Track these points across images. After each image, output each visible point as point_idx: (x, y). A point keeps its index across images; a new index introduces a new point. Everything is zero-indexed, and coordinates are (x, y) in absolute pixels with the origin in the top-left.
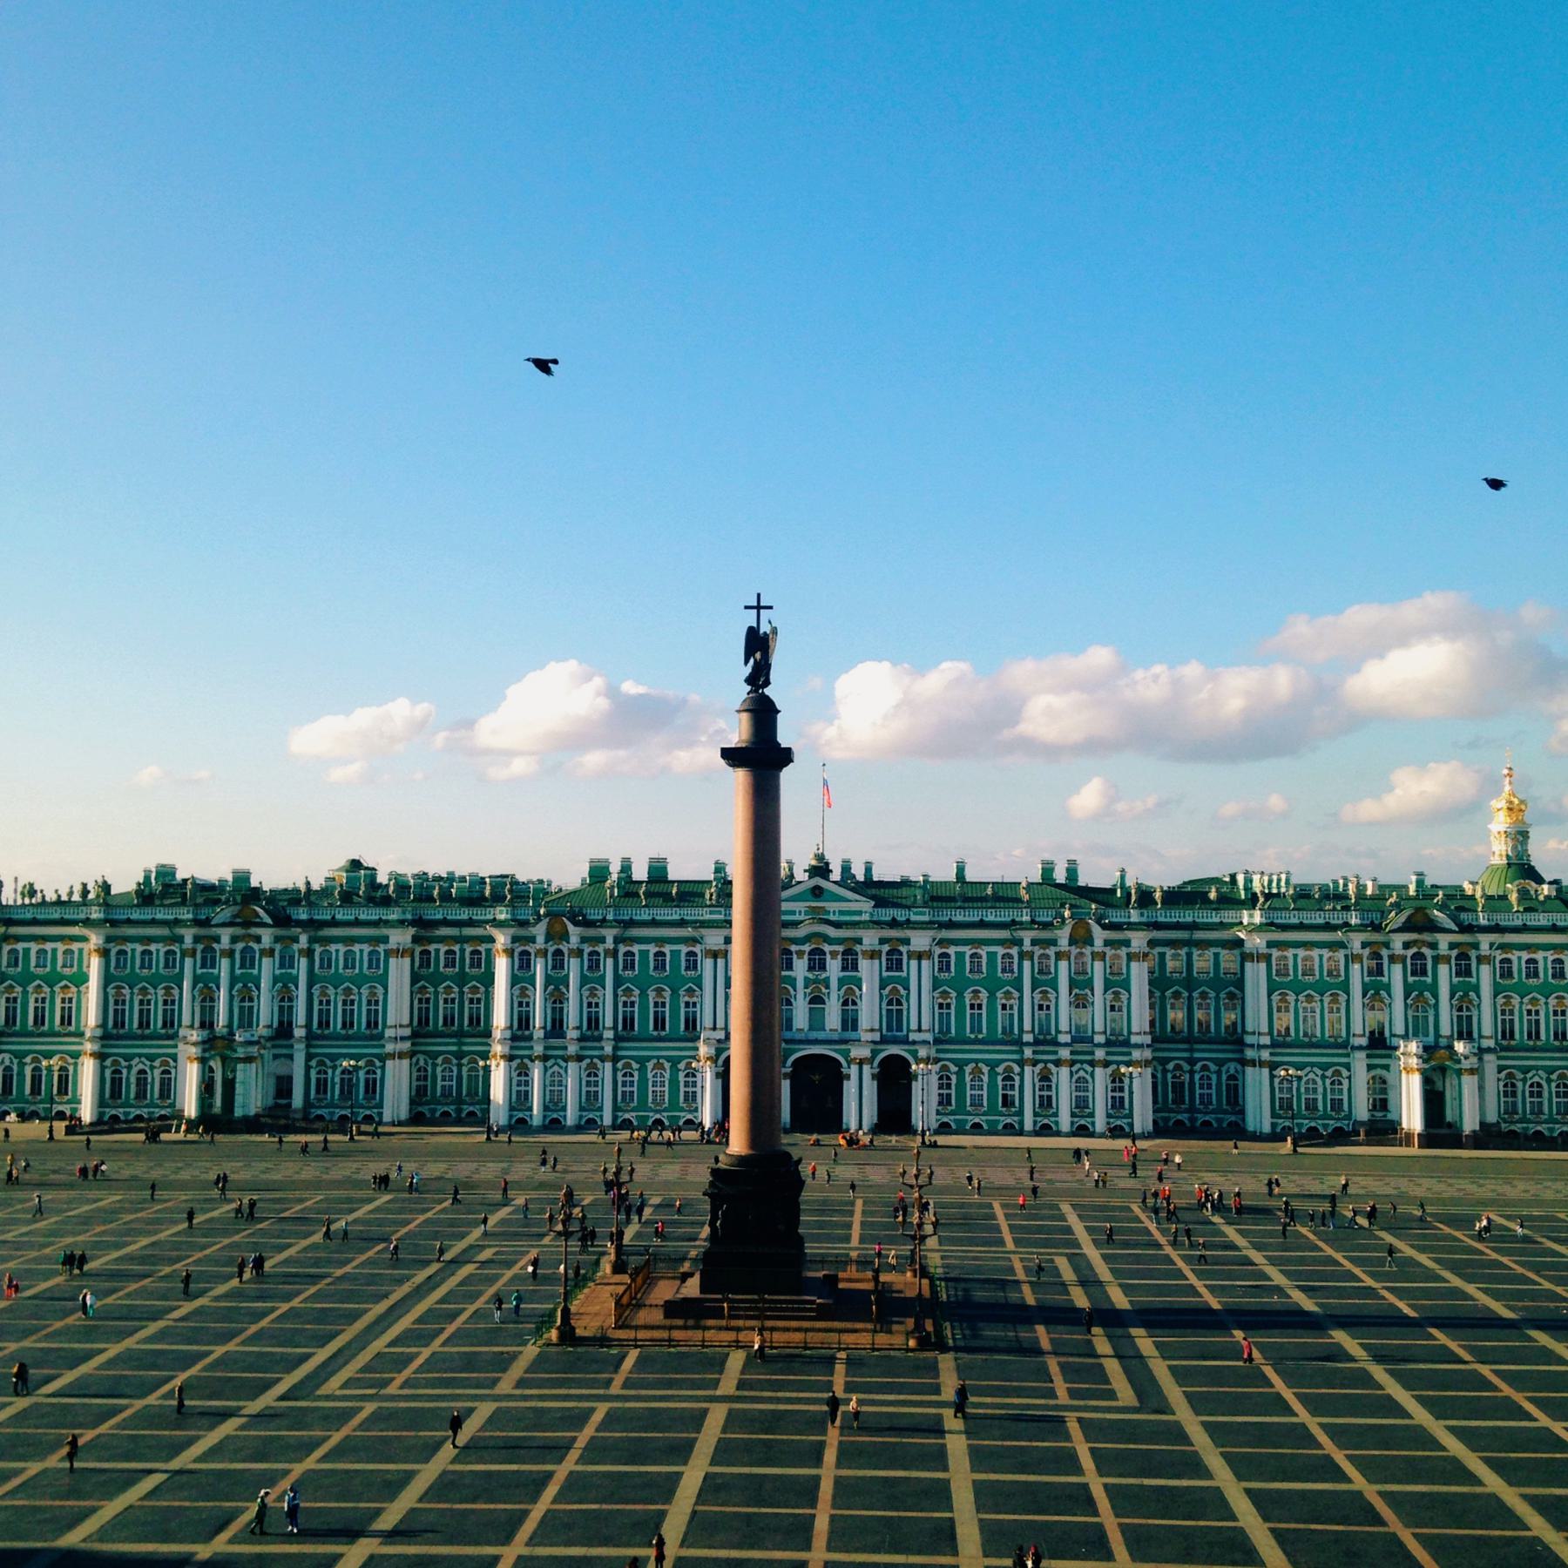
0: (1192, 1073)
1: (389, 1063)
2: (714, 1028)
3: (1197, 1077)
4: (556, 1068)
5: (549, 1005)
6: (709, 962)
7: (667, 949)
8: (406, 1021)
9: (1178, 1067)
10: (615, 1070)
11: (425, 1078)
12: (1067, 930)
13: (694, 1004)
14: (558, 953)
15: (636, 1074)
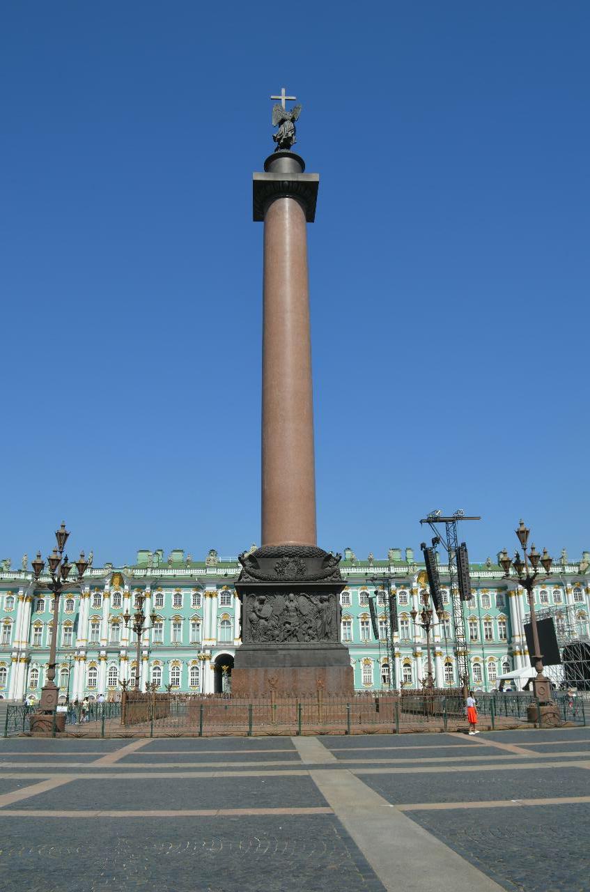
0: (484, 662)
1: (14, 663)
2: (209, 640)
3: (487, 664)
4: (113, 665)
5: (110, 625)
6: (208, 598)
7: (182, 593)
8: (24, 639)
9: (477, 659)
10: (150, 665)
11: (37, 675)
12: (416, 578)
13: (198, 625)
14: (117, 595)
15: (162, 668)
